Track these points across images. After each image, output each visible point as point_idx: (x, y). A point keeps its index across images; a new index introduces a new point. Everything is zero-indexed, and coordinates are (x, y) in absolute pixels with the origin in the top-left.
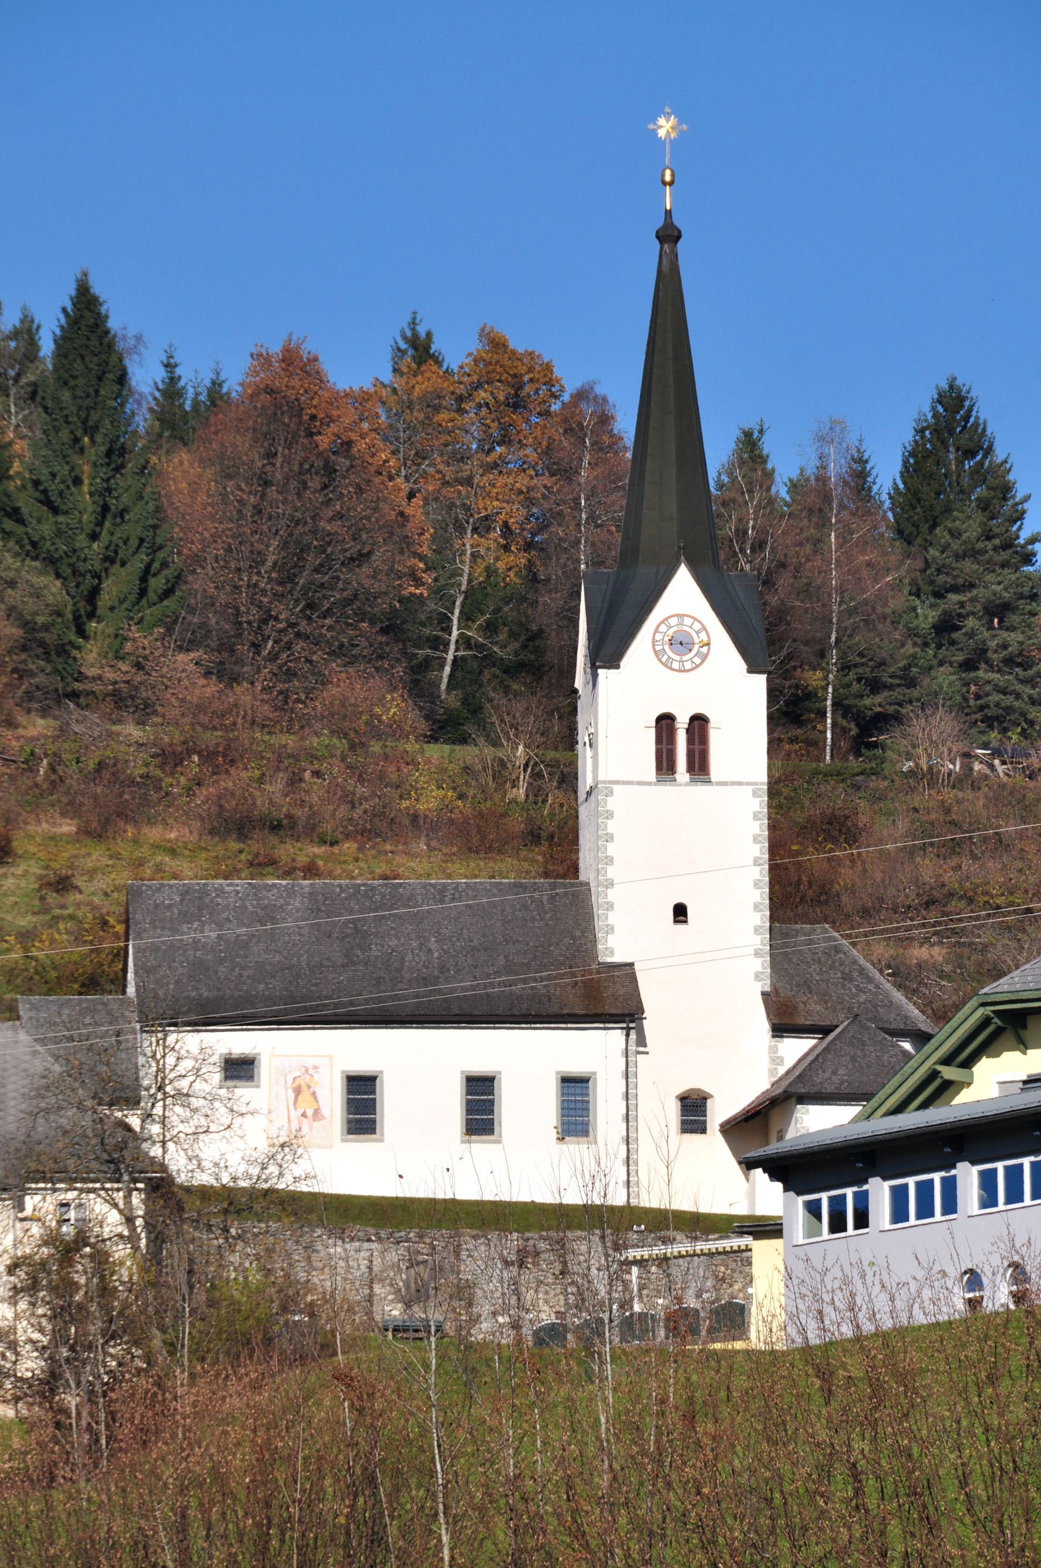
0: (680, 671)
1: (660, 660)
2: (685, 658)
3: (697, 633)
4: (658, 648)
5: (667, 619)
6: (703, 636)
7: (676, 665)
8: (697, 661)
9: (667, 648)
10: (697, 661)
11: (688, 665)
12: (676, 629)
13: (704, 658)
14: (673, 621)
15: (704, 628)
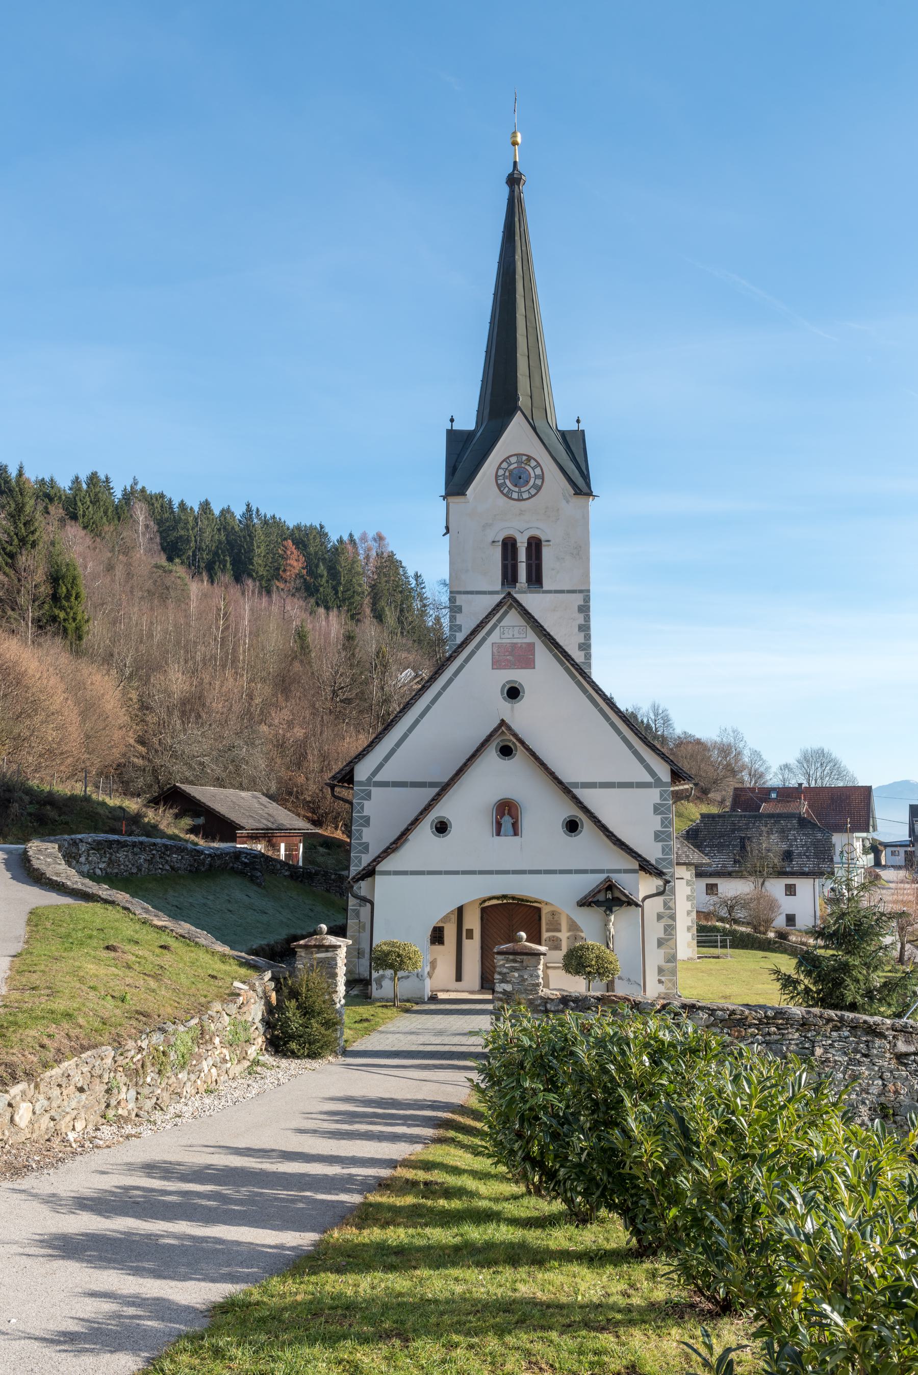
0: (518, 500)
1: (502, 492)
2: (523, 489)
3: (533, 469)
4: (500, 482)
5: (508, 458)
6: (538, 471)
7: (515, 496)
8: (533, 491)
9: (507, 482)
10: (533, 491)
11: (525, 496)
12: (515, 465)
13: (539, 489)
14: (513, 459)
15: (539, 464)
